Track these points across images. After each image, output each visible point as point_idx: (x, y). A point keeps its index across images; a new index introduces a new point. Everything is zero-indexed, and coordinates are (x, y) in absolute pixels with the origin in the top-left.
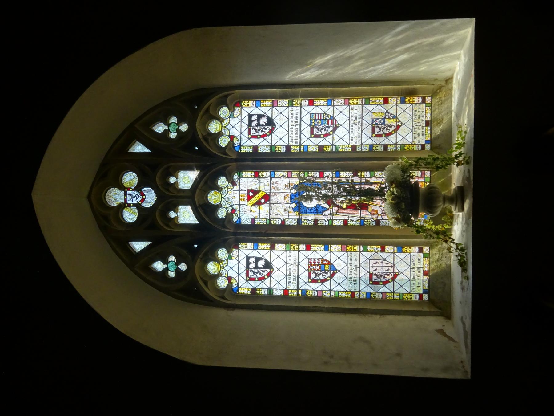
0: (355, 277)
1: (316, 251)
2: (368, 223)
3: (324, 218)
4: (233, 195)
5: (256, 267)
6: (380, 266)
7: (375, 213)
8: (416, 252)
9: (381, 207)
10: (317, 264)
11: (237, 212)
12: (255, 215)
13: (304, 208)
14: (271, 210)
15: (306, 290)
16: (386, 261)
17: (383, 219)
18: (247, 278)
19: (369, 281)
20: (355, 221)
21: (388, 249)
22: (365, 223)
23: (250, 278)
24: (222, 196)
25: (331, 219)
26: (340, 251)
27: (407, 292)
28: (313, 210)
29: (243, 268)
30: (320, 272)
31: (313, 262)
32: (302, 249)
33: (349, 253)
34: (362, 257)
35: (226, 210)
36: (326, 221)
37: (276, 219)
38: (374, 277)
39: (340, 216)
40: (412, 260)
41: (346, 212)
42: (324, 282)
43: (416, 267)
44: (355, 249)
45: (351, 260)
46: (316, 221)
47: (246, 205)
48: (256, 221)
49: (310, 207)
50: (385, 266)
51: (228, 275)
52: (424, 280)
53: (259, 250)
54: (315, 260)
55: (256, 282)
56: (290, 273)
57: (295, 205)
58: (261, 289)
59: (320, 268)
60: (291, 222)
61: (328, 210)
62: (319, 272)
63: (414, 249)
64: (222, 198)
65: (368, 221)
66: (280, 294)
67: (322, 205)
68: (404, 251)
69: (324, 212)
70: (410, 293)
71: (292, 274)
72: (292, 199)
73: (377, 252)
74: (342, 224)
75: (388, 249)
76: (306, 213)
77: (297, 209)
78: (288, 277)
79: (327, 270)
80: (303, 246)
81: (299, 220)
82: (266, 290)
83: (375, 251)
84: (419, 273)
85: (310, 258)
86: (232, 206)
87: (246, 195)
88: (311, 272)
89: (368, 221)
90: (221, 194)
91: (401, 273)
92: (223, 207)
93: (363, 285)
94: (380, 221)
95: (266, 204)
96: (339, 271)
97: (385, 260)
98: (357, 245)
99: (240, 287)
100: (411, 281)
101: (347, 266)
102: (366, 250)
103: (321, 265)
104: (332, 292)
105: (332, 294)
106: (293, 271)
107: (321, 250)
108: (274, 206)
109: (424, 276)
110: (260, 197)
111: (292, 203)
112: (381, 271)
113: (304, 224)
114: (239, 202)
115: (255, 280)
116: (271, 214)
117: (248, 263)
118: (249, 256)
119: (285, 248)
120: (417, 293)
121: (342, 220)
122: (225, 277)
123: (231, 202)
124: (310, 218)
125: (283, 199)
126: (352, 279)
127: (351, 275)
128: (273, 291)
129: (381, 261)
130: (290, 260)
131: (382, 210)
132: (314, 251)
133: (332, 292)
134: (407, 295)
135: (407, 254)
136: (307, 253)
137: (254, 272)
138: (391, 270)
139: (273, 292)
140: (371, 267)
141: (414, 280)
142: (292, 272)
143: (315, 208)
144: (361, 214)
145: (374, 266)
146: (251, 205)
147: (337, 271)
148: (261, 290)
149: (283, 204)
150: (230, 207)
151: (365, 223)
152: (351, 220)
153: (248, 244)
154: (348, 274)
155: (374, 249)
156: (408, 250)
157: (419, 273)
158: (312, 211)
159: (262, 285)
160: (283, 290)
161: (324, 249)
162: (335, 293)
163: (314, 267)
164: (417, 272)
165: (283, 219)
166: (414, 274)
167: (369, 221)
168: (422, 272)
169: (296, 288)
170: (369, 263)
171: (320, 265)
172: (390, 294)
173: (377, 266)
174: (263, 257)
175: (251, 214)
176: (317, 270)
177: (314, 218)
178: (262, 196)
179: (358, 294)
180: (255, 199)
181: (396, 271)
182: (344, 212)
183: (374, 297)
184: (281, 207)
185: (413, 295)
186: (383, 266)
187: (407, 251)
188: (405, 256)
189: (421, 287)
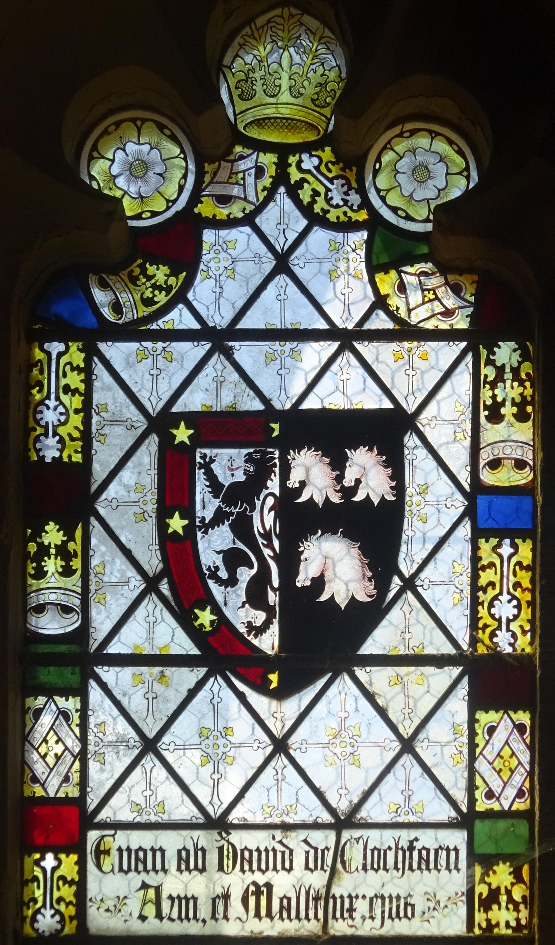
53: (468, 549)
55: (152, 521)
58: (76, 564)
66: (40, 769)
106: (269, 886)
119: (496, 807)
128: (66, 693)
142: (261, 879)
148: (67, 572)
160: (74, 792)
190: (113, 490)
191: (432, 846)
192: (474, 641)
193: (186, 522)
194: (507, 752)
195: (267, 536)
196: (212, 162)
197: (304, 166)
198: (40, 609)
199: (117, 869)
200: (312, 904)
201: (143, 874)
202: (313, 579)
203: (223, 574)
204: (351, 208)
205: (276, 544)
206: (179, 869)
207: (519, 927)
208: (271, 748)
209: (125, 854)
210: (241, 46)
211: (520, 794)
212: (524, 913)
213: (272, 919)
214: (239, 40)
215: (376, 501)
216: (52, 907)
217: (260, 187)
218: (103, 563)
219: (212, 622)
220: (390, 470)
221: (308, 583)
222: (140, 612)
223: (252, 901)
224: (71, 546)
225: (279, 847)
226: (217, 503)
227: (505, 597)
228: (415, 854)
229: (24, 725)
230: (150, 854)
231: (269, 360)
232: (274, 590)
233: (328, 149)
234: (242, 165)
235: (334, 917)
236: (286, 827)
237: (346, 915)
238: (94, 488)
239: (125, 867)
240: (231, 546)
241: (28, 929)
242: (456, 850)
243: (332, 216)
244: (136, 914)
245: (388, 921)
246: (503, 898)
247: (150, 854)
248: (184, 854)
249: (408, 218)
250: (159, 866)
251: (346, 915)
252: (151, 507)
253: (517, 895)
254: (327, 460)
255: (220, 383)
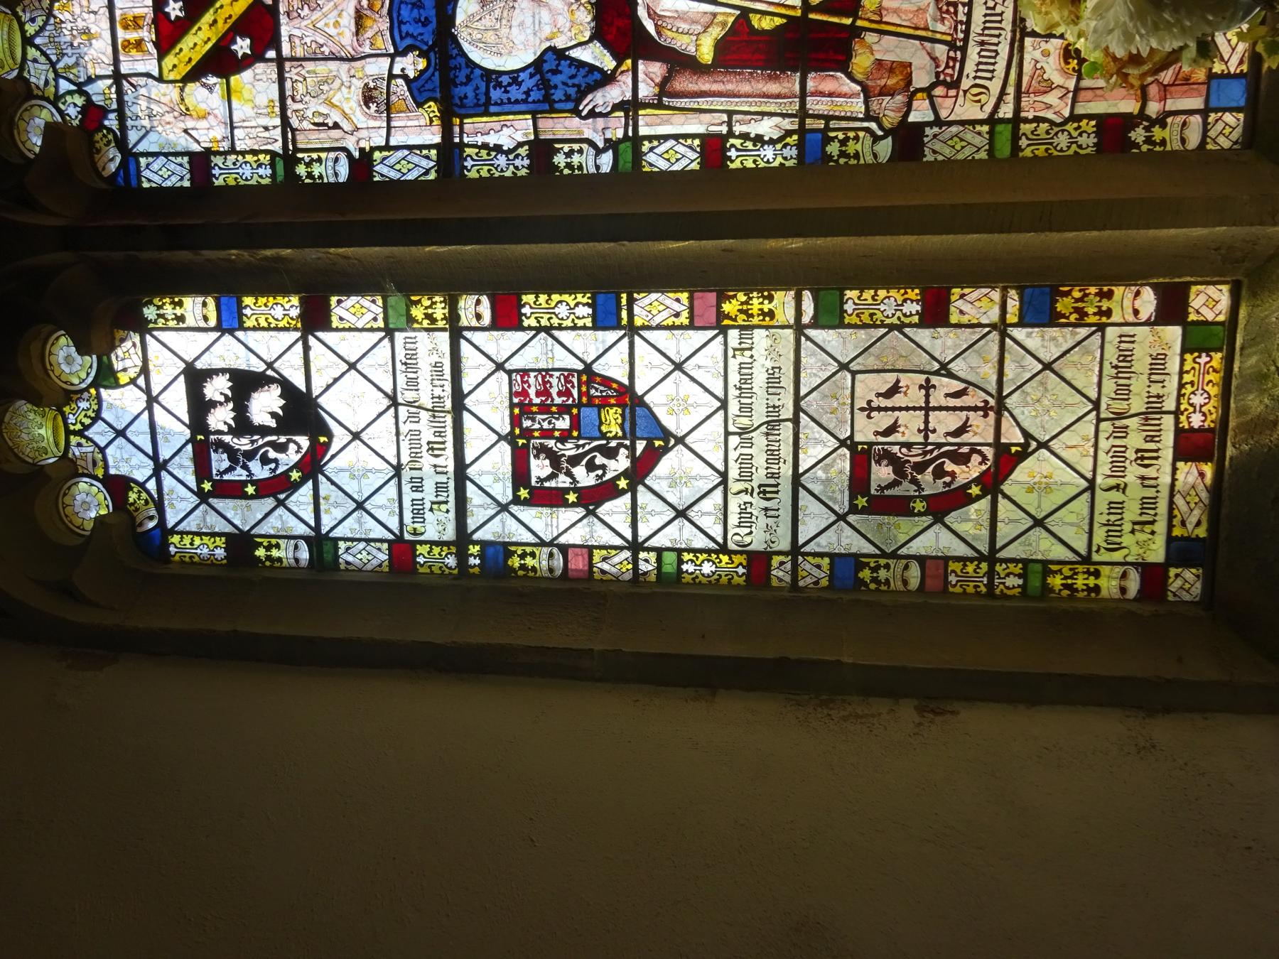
0: (773, 476)
1: (548, 330)
2: (852, 147)
3: (589, 130)
4: (80, 24)
5: (243, 425)
6: (914, 409)
7: (891, 82)
8: (1143, 316)
9: (928, 45)
10: (558, 400)
11: (112, 121)
12: (209, 134)
13: (469, 79)
14: (293, 100)
15: (505, 545)
16: (951, 375)
17: (938, 122)
18: (199, 481)
19: (847, 493)
20: (772, 142)
21: (966, 308)
22: (833, 149)
23: (216, 484)
24: (23, 32)
25: (630, 134)
26: (681, 327)
27: (1070, 556)
28: (524, 88)
29: (175, 430)
30: (578, 447)
31: (538, 394)
32: (474, 323)
33: (733, 334)
34: (812, 360)
35: (54, 111)
36: (599, 152)
37: (323, 155)
38: (882, 473)
39: (679, 118)
40: (1108, 370)
41: (716, 87)
42: (599, 505)
43: (1132, 412)
44: (771, 314)
45: (746, 379)
46: (541, 149)
47: (156, 73)
48: (216, 172)
49: (509, 67)
50: (947, 409)
51: (106, 467)
52: (1179, 485)
53: (249, 333)
54: (545, 383)
55: (250, 502)
56: (415, 457)
57: (422, 64)
58: (274, 541)
59: (576, 423)
60: (404, 166)
61: (607, 79)
62: (569, 446)
63: (1127, 304)
64: (28, 41)
65: (847, 139)
66: (375, 562)
67: (574, 54)
68: (1064, 316)
69: (590, 97)
70: (1086, 560)
71: (427, 461)
72: (401, 23)
73: (900, 327)
74: (695, 166)
75: (966, 308)
76: (484, 108)
77: (428, 87)
78: (406, 474)
79: (615, 437)
80: (478, 302)
81: (449, 152)
82: (303, 545)
83: (888, 321)
84: (1152, 446)
85: (517, 371)
86: (79, 85)
87: (149, 20)
88: (526, 446)
89: (847, 139)
90: (18, 18)
91: (1043, 445)
92: (38, 97)
93: (813, 519)
94: (923, 135)
95: (260, 67)
96: (680, 440)
97: (945, 370)
98: (784, 285)
99: (173, 531)
100: (1098, 492)
101: (721, 413)
102: (831, 317)
103: (579, 405)
104: (642, 555)
105: (643, 567)
106: (429, 443)
107: (580, 323)
108: (303, 72)
109: (1180, 464)
110: (227, 26)
111: (403, 53)
112: (920, 439)
113: (477, 176)
114: (116, 62)
115: (245, 496)
116: (295, 122)
117: (199, 407)
118: (199, 365)
119: (381, 316)
120: (1129, 559)
121: (693, 136)
122: (95, 478)
123: (77, 64)
124: (505, 138)
125: (354, 30)
126: (755, 484)
127: (744, 462)
128: (337, 548)
129: (921, 378)
130: (413, 384)
131: (935, 59)
132: (539, 329)
133: (642, 555)
134: (1069, 574)
135: (1083, 332)
136: (503, 343)
137: (232, 453)
138: (981, 431)
139: (337, 557)
140: (860, 418)
141: (1117, 487)
142: (425, 447)
143: (531, 76)
144: (803, 95)
145: (879, 409)
146: (179, 78)
147: (667, 441)
148: (278, 546)
149: (353, 59)
150: (70, 93)
151: (829, 149)
152: (745, 136)
153: (188, 301)
154: (733, 455)
155: (882, 307)
156: (1091, 310)
157: (1152, 446)
158: (516, 93)
159: (279, 522)
160: (385, 546)
161: (594, 317)
162: (659, 560)
163: (542, 422)
164: (1135, 440)
165: (362, 150)
166: (1118, 456)
167: (857, 138)
168: (1168, 439)
169: (450, 534)
170: (848, 392)
171: (575, 411)
172: (970, 568)
173: (900, 409)
174: (270, 373)
175: (186, 131)
176: (557, 434)
177: (532, 137)
178: (234, 18)
179: (788, 566)
180: (196, 39)
181: (1012, 436)
182: (706, 87)
183: (875, 580)
184: (345, 78)
185: (1105, 570)
186: (935, 409)
187: (1087, 314)
188: (1070, 343)
189: (1161, 527)
190: (237, 522)
191: (404, 352)
192: (296, 329)
193: (249, 485)
194: (352, 310)
195: (252, 442)
196: (77, 469)
197: (74, 422)
198: (297, 560)
199: (423, 525)
200: (437, 419)
201: (425, 511)
202: (272, 418)
203: (273, 466)
204: (90, 397)
205: (256, 437)
206: (422, 491)
207: (444, 301)
208: (357, 441)
209: (416, 520)
210: (23, 454)
211: (374, 302)
212: (437, 299)
213: (445, 441)
214: (20, 455)
215: (230, 384)
216: (444, 559)
217: (87, 445)
218: (273, 528)
219: (297, 472)
220: (214, 376)
221: (274, 421)
222: (295, 509)
223: (436, 452)
224: (265, 544)
225: (409, 437)
226: (238, 468)
227: (272, 312)
228: (408, 361)
229: (354, 570)
230: (415, 507)
231: (167, 441)
232: (279, 439)
233: (64, 409)
234: (77, 453)
235: (443, 407)
236: (398, 434)
237: (442, 400)
238: (237, 532)
239: (422, 520)
240: (259, 461)
241: (456, 572)
242: (406, 338)
243: (96, 407)
244: (446, 515)
245: (445, 377)
246: (430, 311)
247: (415, 507)
248: (414, 489)
249: (91, 367)
250: (421, 502)
251: (442, 400)
252: (244, 502)
253: (428, 303)
254: (212, 410)
255: (181, 466)
